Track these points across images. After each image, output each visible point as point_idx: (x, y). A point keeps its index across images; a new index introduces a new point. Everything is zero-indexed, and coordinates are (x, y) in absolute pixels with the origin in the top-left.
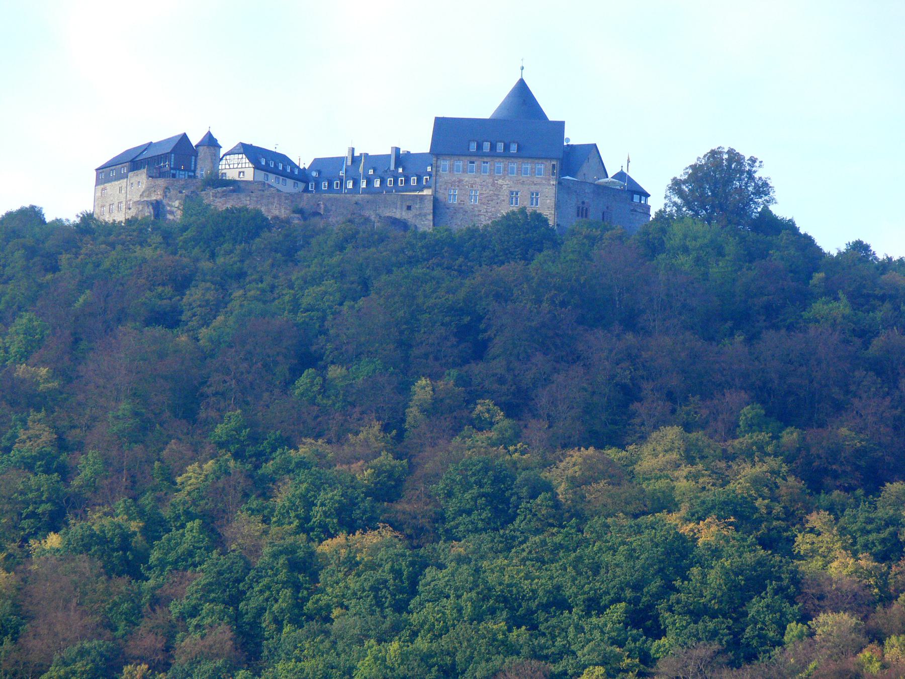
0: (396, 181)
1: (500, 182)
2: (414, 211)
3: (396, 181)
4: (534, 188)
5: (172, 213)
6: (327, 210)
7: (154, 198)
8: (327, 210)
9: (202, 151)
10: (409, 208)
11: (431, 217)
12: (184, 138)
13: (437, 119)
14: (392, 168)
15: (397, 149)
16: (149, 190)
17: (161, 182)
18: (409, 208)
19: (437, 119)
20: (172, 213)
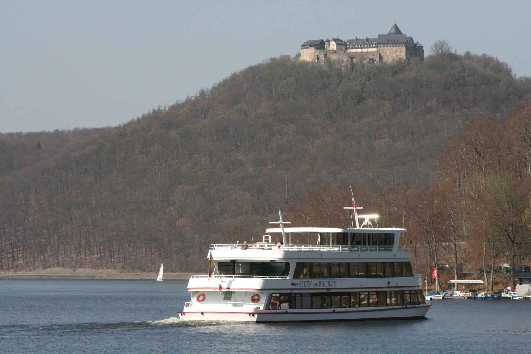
0: (367, 45)
1: (393, 48)
2: (375, 56)
3: (367, 45)
4: (401, 50)
5: (321, 57)
6: (356, 56)
7: (317, 54)
8: (356, 56)
9: (326, 43)
10: (374, 55)
11: (379, 57)
12: (322, 40)
13: (378, 35)
14: (366, 42)
15: (367, 38)
16: (315, 52)
17: (318, 50)
18: (374, 55)
19: (378, 35)
20: (321, 57)
